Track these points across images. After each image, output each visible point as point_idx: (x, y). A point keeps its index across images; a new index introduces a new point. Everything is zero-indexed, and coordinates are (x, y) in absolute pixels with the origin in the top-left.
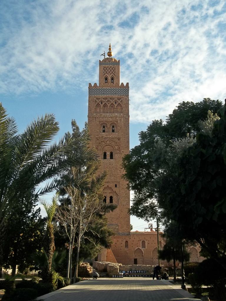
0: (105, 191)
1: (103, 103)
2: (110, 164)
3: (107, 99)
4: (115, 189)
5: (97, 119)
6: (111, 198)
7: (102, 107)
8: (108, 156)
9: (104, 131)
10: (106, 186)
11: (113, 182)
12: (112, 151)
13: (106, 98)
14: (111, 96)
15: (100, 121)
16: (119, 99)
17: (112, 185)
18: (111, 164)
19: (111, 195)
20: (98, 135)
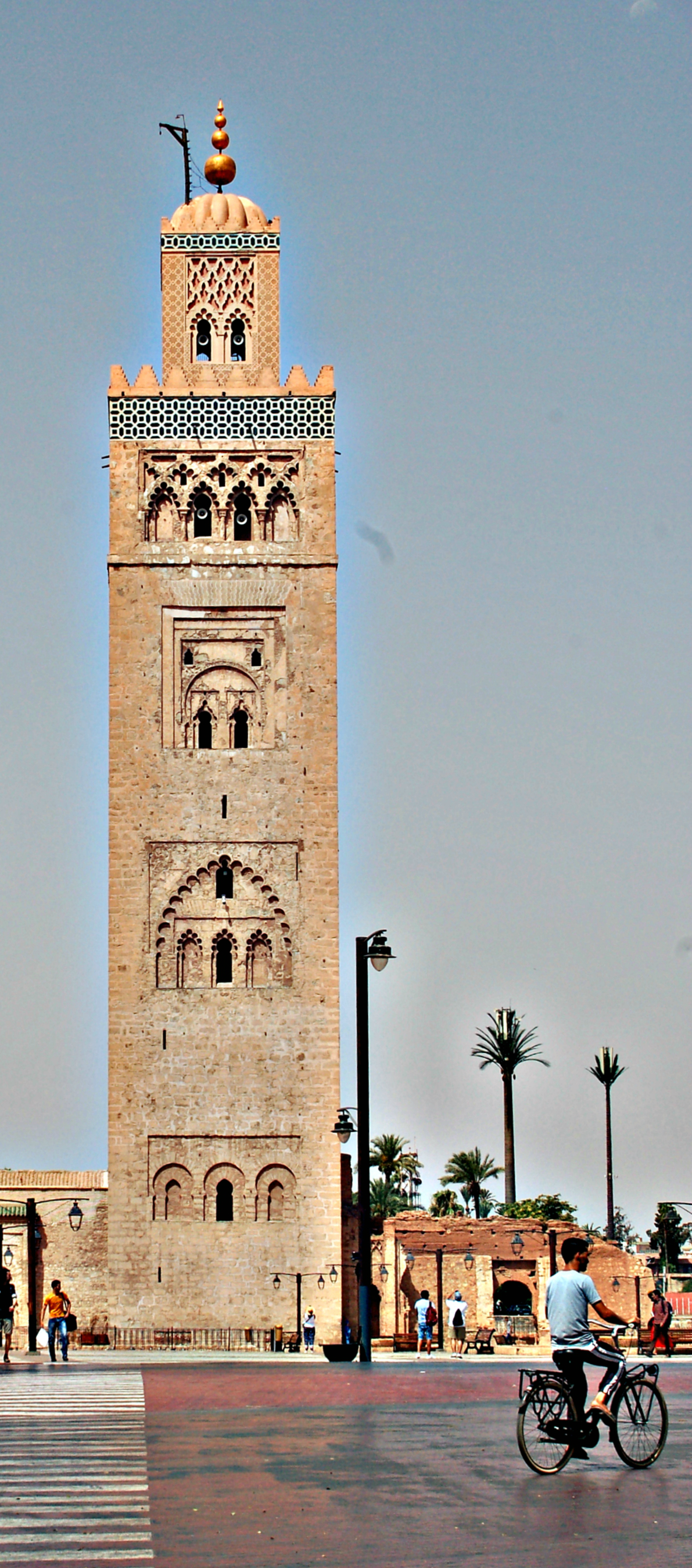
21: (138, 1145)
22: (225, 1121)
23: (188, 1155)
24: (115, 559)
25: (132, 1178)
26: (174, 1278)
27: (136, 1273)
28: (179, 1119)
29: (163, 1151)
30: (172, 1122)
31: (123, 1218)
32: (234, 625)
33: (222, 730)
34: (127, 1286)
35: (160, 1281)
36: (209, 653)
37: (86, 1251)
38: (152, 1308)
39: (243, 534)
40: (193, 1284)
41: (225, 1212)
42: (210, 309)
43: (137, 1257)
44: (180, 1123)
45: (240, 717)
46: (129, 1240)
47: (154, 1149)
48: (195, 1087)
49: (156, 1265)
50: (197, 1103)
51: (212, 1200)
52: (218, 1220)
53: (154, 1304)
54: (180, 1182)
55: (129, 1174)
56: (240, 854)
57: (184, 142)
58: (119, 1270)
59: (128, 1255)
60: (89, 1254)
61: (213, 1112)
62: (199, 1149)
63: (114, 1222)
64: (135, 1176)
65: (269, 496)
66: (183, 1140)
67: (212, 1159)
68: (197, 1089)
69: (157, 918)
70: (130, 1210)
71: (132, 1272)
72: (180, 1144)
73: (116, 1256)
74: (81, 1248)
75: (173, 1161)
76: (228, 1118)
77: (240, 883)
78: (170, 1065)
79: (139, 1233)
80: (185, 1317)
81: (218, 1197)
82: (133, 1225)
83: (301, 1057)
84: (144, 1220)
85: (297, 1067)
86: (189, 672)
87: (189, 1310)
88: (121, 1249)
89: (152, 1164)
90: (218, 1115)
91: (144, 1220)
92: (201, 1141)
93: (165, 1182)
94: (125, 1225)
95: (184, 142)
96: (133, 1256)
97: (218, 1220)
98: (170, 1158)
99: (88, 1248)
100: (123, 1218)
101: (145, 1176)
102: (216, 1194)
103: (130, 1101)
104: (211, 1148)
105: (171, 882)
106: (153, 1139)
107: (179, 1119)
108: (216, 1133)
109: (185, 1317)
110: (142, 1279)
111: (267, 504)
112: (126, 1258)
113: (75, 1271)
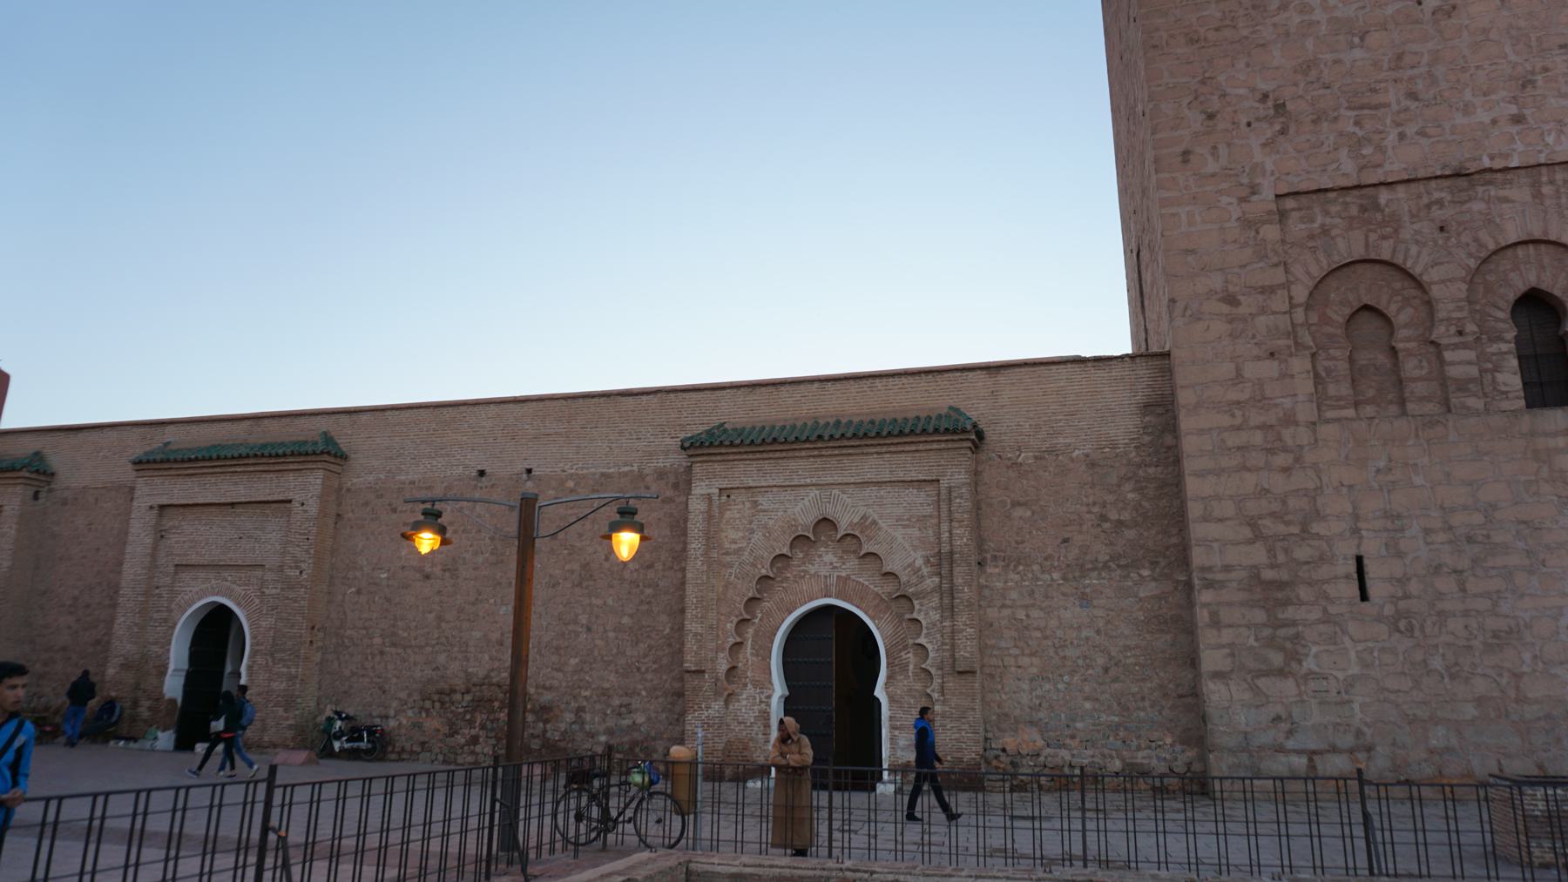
21: (1247, 223)
22: (1514, 129)
23: (1406, 234)
25: (1242, 310)
26: (1414, 587)
27: (1284, 575)
28: (1361, 142)
29: (1325, 231)
30: (1344, 152)
31: (1226, 420)
34: (1259, 616)
35: (1364, 597)
37: (1120, 523)
38: (1350, 684)
40: (1483, 604)
43: (1282, 529)
44: (1367, 151)
46: (1250, 479)
47: (1297, 228)
48: (1400, 57)
49: (1345, 551)
50: (1413, 96)
52: (1530, 405)
53: (1355, 670)
54: (1391, 311)
55: (1232, 300)
58: (1227, 568)
59: (1252, 523)
60: (1130, 534)
61: (1467, 109)
62: (1436, 213)
63: (1201, 432)
64: (1248, 305)
66: (1384, 196)
67: (1484, 236)
68: (1407, 59)
70: (1244, 396)
71: (1268, 574)
72: (1377, 207)
73: (1213, 530)
74: (1103, 518)
75: (1359, 252)
76: (1518, 119)
78: (1318, 15)
79: (1281, 460)
80: (1470, 711)
81: (1518, 340)
82: (1258, 438)
84: (1290, 420)
87: (1480, 686)
88: (1228, 509)
89: (1298, 270)
90: (1484, 117)
91: (1290, 420)
92: (1439, 192)
93: (1339, 315)
94: (1233, 440)
96: (1269, 526)
97: (1530, 405)
98: (1350, 245)
99: (1126, 516)
100: (1226, 420)
101: (1279, 302)
102: (1511, 334)
103: (1211, 116)
104: (1477, 206)
106: (1290, 203)
107: (1361, 142)
108: (1487, 163)
109: (1470, 711)
110: (1304, 592)
112: (1247, 532)
113: (1092, 580)
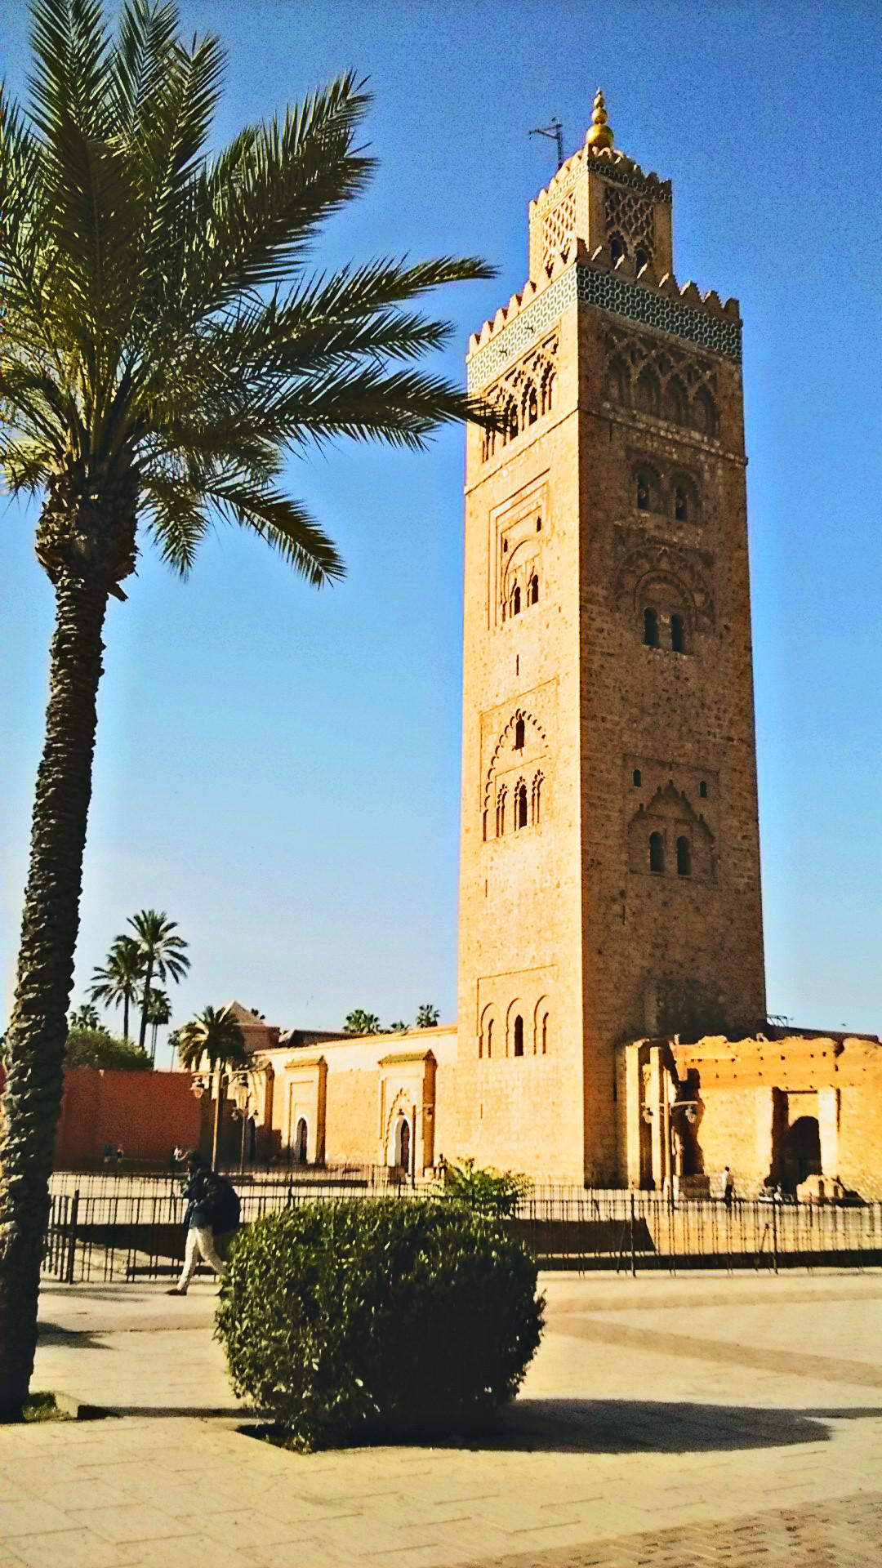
0: (662, 809)
1: (642, 364)
2: (678, 678)
3: (654, 346)
4: (702, 808)
5: (617, 434)
6: (682, 844)
7: (635, 378)
8: (666, 641)
9: (643, 504)
10: (664, 783)
11: (692, 769)
12: (683, 614)
13: (650, 341)
14: (672, 340)
15: (629, 450)
16: (707, 365)
17: (685, 783)
18: (683, 676)
19: (683, 830)
20: (622, 517)
24: (466, 490)
32: (524, 503)
33: (523, 596)
36: (514, 537)
39: (533, 419)
41: (519, 1052)
42: (552, 251)
45: (535, 581)
51: (512, 1035)
56: (526, 705)
57: (558, 137)
65: (544, 379)
69: (485, 780)
77: (530, 731)
83: (558, 886)
85: (555, 895)
86: (507, 556)
95: (558, 137)
105: (491, 741)
111: (543, 386)
